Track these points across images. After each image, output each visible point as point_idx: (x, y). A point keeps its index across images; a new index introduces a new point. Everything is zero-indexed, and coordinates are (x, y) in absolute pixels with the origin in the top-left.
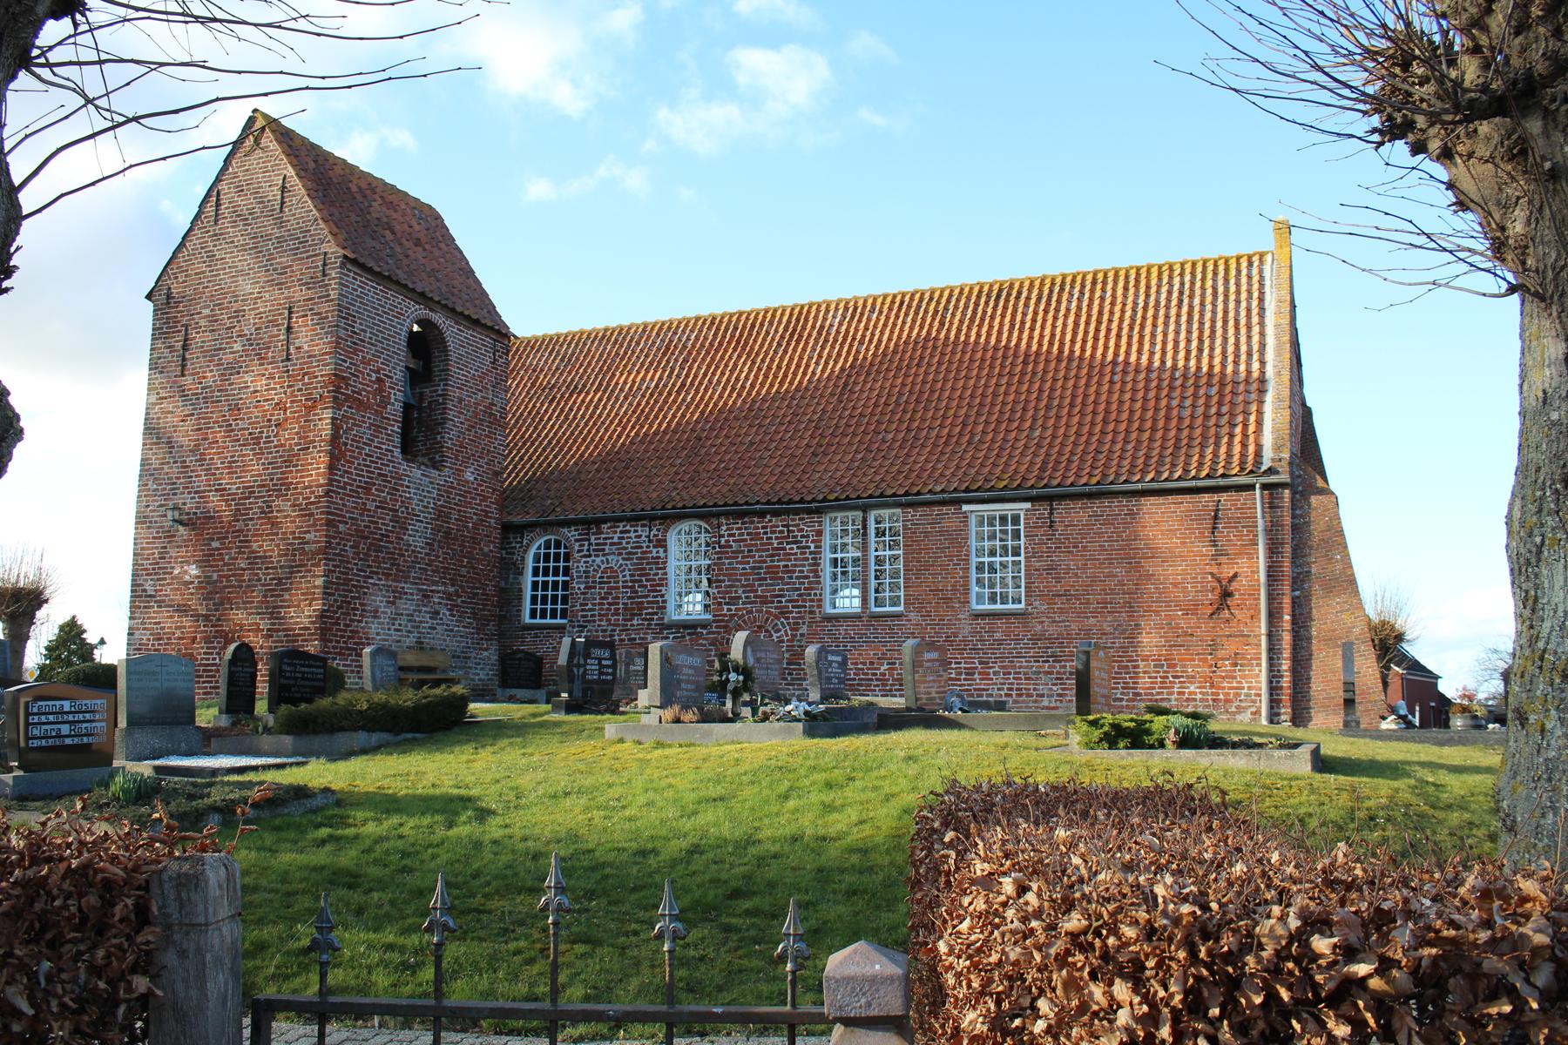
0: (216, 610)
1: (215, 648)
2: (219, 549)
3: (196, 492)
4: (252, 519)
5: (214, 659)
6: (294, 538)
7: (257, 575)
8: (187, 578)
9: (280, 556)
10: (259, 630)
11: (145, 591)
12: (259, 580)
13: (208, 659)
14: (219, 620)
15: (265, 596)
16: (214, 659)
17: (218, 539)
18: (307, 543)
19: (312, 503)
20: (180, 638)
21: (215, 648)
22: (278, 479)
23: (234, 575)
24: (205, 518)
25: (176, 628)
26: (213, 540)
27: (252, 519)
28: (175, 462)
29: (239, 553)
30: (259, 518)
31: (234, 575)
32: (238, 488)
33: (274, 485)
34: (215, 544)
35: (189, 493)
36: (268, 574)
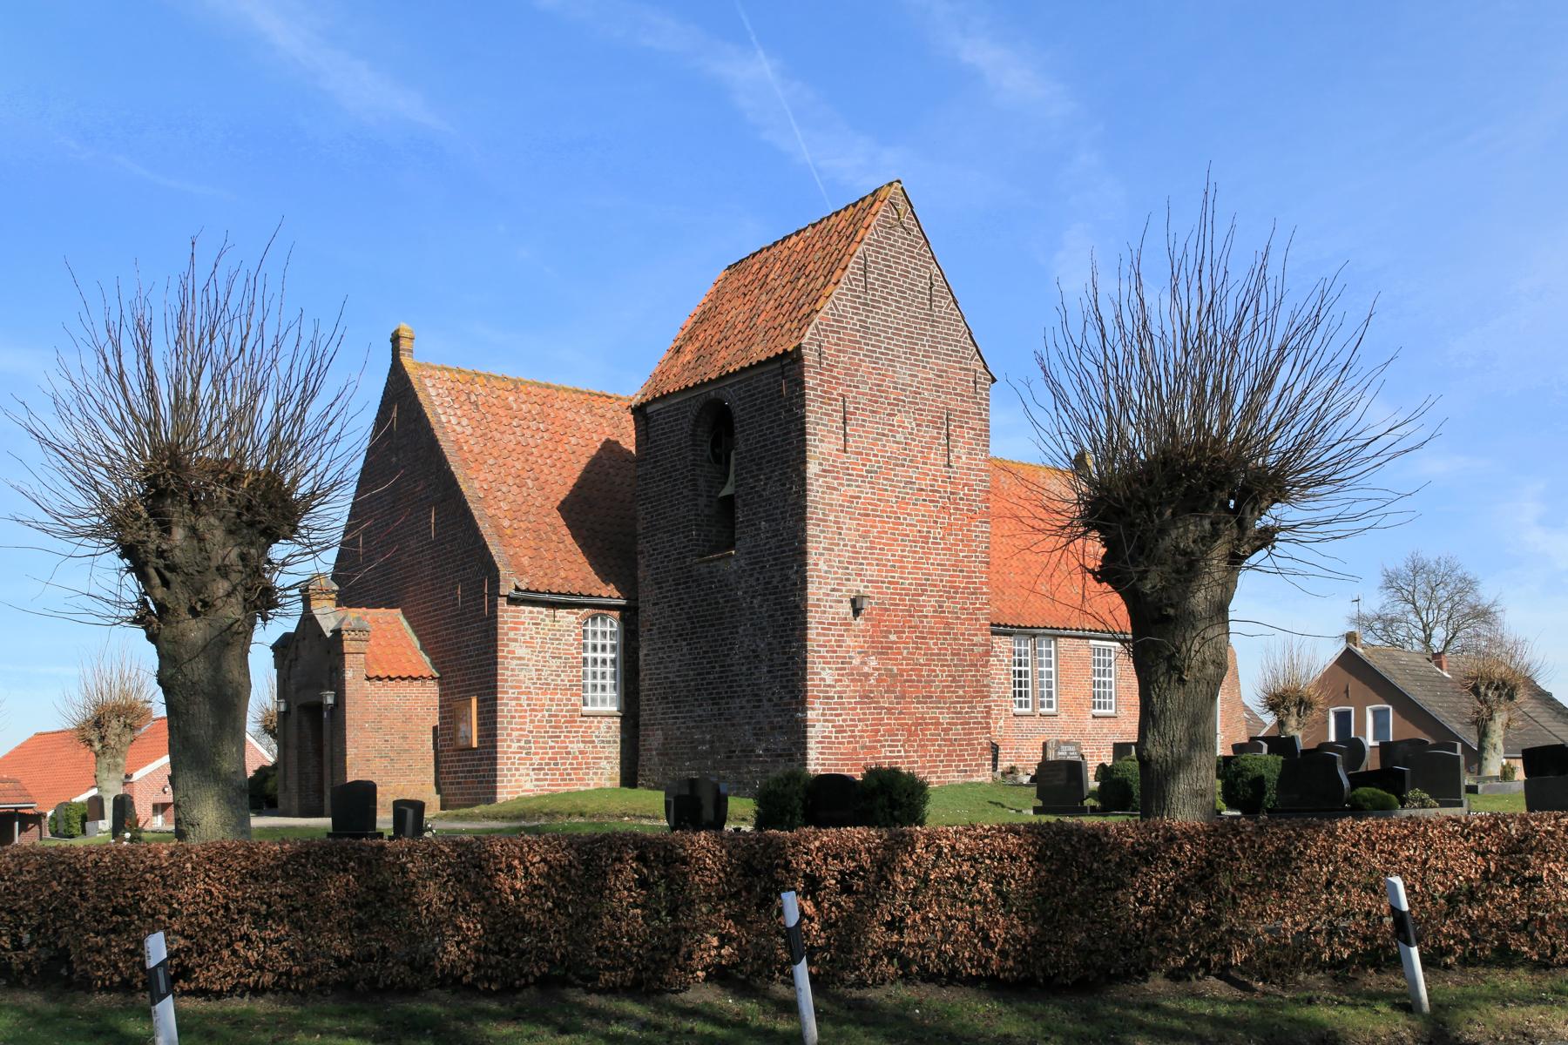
0: (898, 703)
1: (899, 741)
2: (896, 643)
3: (869, 581)
4: (926, 617)
5: (899, 751)
6: (964, 639)
7: (935, 671)
8: (866, 669)
9: (953, 654)
10: (939, 724)
11: (824, 680)
12: (937, 676)
13: (893, 752)
14: (899, 714)
15: (942, 692)
16: (899, 751)
17: (895, 632)
18: (975, 645)
19: (979, 609)
20: (863, 731)
21: (899, 741)
22: (947, 581)
23: (912, 670)
24: (881, 609)
25: (860, 720)
26: (890, 632)
27: (926, 617)
28: (845, 545)
29: (917, 648)
30: (933, 617)
31: (912, 670)
32: (911, 584)
33: (943, 586)
34: (893, 637)
35: (862, 581)
36: (944, 671)
